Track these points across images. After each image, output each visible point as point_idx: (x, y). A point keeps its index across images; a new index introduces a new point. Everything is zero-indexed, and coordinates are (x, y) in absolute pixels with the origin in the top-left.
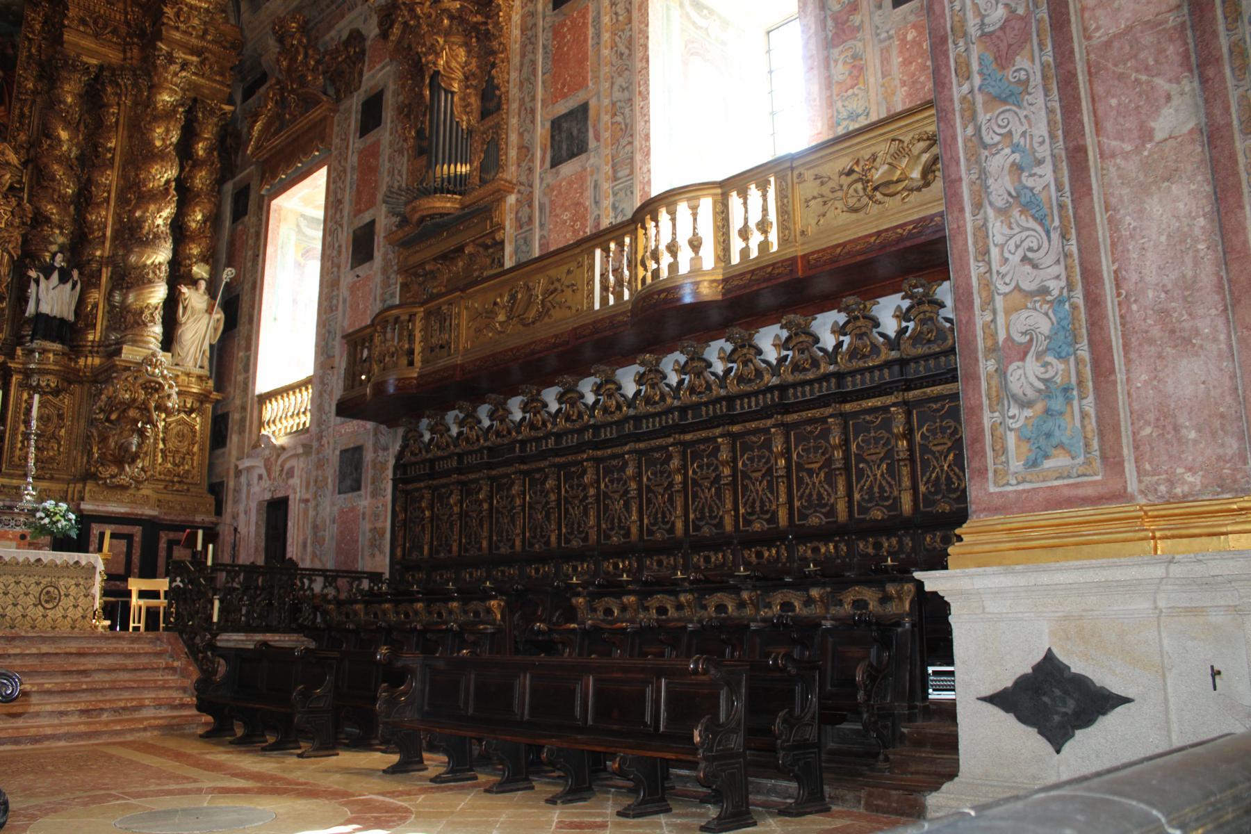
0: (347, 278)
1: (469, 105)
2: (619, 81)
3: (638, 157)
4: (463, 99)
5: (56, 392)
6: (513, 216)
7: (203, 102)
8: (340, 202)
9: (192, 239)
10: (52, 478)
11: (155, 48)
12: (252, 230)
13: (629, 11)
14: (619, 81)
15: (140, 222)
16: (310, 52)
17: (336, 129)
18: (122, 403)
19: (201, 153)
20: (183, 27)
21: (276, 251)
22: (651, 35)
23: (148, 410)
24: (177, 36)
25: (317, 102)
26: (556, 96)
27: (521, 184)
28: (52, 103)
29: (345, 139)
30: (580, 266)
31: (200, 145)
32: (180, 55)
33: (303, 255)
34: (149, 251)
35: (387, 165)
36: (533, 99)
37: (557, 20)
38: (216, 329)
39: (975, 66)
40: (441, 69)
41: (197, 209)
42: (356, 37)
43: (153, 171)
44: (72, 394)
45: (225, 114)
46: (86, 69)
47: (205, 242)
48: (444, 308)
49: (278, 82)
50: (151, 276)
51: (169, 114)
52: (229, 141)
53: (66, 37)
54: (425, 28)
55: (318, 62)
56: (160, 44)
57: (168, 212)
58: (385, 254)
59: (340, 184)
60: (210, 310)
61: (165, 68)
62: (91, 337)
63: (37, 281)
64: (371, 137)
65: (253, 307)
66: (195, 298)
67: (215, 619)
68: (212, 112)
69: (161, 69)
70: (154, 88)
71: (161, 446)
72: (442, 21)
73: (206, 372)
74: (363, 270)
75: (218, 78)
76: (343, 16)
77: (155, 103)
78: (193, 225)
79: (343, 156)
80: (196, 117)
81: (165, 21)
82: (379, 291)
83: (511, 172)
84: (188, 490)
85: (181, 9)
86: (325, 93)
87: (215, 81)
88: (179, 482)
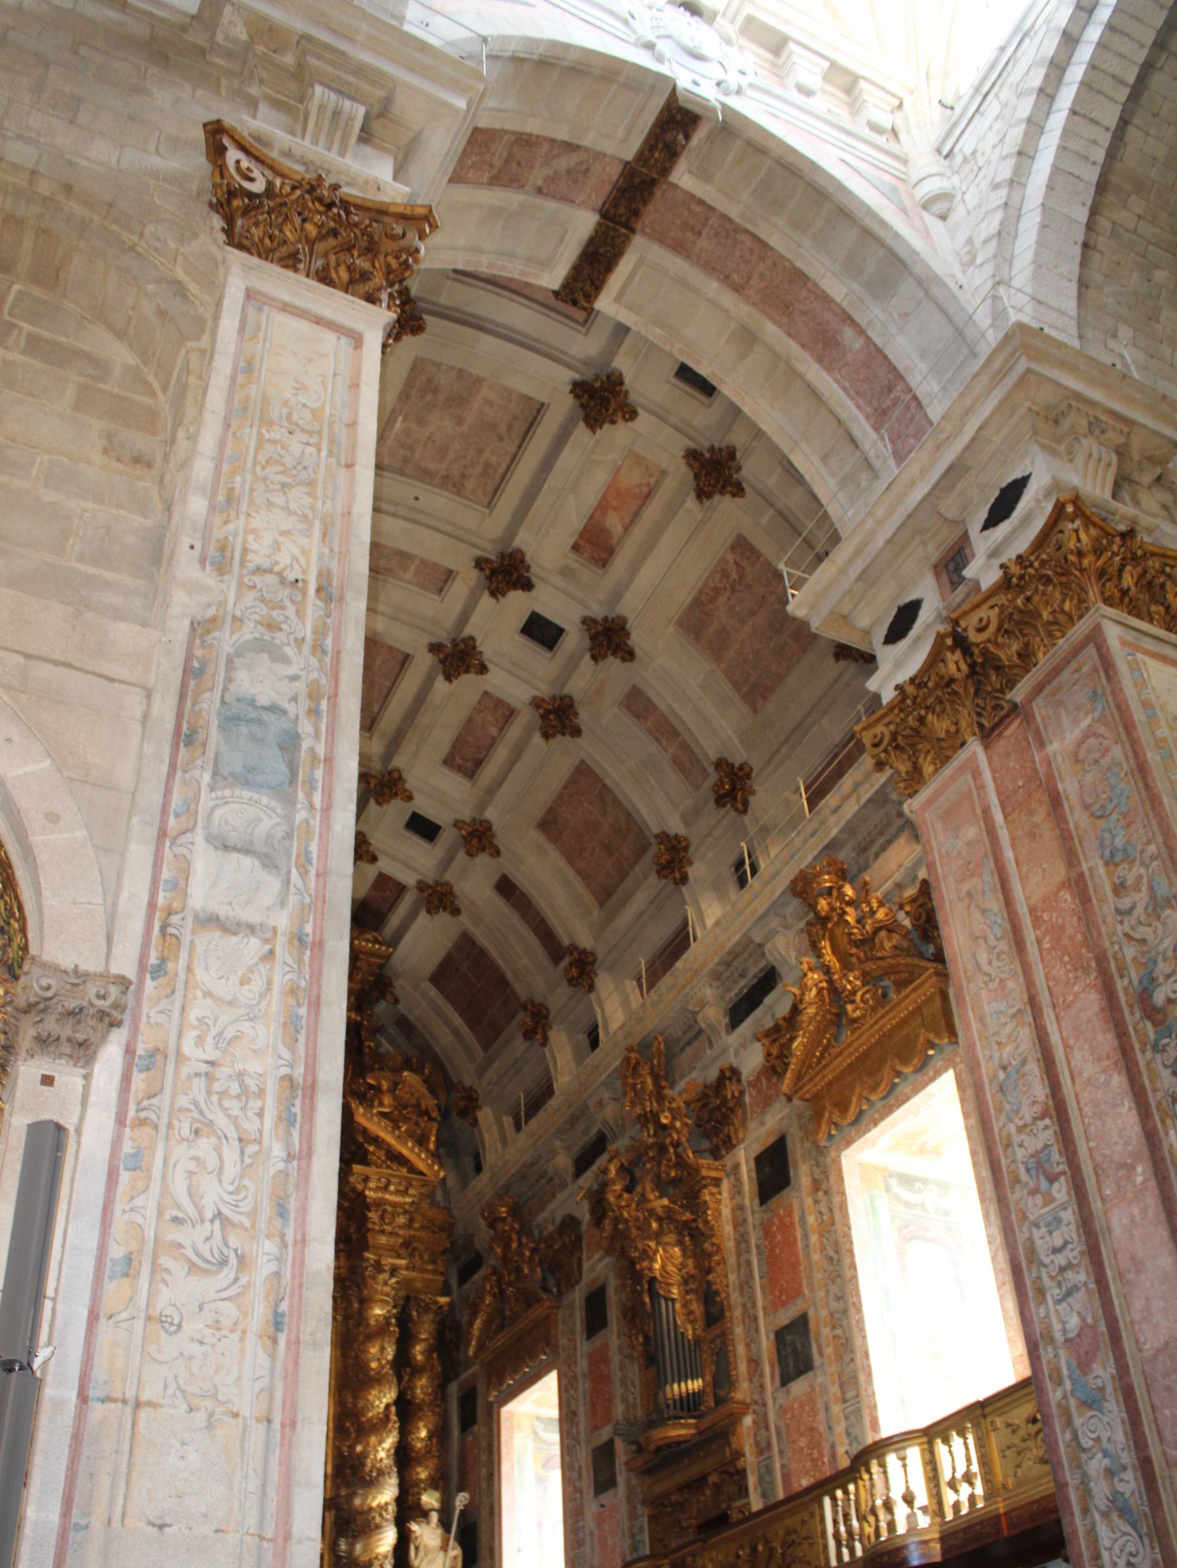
0: (591, 1508)
1: (690, 1312)
2: (834, 1289)
3: (862, 1377)
4: (684, 1306)
6: (751, 1440)
7: (416, 1298)
8: (574, 1414)
9: (419, 1463)
11: (363, 1259)
12: (484, 1443)
13: (831, 1210)
14: (834, 1289)
15: (363, 1456)
16: (524, 1240)
17: (561, 1327)
19: (419, 1357)
20: (388, 1228)
21: (512, 1468)
22: (855, 1239)
24: (383, 1240)
25: (538, 1300)
26: (776, 1304)
27: (756, 1403)
29: (572, 1340)
30: (812, 1515)
31: (418, 1348)
32: (388, 1261)
33: (544, 1466)
34: (373, 1491)
35: (618, 1374)
36: (754, 1306)
37: (766, 1216)
39: (1065, 1372)
40: (657, 1274)
41: (421, 1424)
42: (570, 1223)
43: (371, 1398)
45: (441, 1307)
47: (432, 1463)
48: (689, 1559)
49: (495, 1271)
50: (378, 1520)
51: (382, 1331)
52: (448, 1336)
54: (634, 1232)
55: (534, 1251)
56: (367, 1255)
57: (390, 1441)
58: (628, 1480)
59: (572, 1392)
60: (444, 1548)
61: (373, 1278)
64: (598, 1341)
65: (492, 1537)
66: (427, 1534)
68: (427, 1308)
69: (370, 1281)
70: (365, 1302)
72: (650, 1226)
74: (607, 1498)
75: (430, 1267)
76: (554, 1196)
77: (367, 1320)
78: (419, 1445)
79: (571, 1361)
80: (411, 1316)
81: (370, 1226)
82: (626, 1524)
83: (743, 1391)
85: (385, 1211)
86: (546, 1289)
87: (427, 1271)
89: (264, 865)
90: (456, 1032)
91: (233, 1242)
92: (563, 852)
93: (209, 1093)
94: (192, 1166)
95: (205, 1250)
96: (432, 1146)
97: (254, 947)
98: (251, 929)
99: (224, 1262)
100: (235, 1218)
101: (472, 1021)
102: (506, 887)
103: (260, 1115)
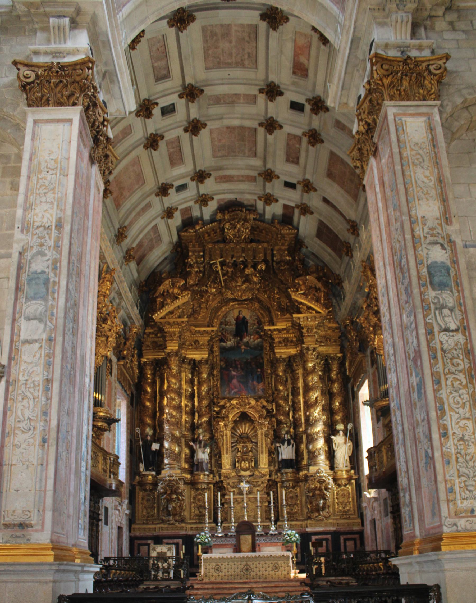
5: (293, 487)
7: (330, 356)
10: (297, 520)
18: (312, 489)
23: (322, 490)
24: (309, 339)
28: (277, 375)
38: (350, 449)
44: (300, 486)
45: (340, 358)
46: (284, 360)
47: (341, 415)
51: (313, 370)
53: (276, 351)
56: (303, 346)
60: (345, 443)
61: (307, 353)
62: (303, 463)
63: (280, 447)
66: (339, 439)
67: (314, 573)
71: (336, 501)
73: (349, 468)
84: (349, 517)
88: (346, 515)
89: (40, 322)
90: (330, 254)
91: (32, 424)
92: (339, 185)
93: (26, 388)
94: (22, 407)
95: (26, 427)
96: (322, 302)
97: (37, 345)
98: (36, 341)
99: (30, 429)
100: (32, 418)
101: (334, 249)
102: (325, 200)
103: (39, 391)
